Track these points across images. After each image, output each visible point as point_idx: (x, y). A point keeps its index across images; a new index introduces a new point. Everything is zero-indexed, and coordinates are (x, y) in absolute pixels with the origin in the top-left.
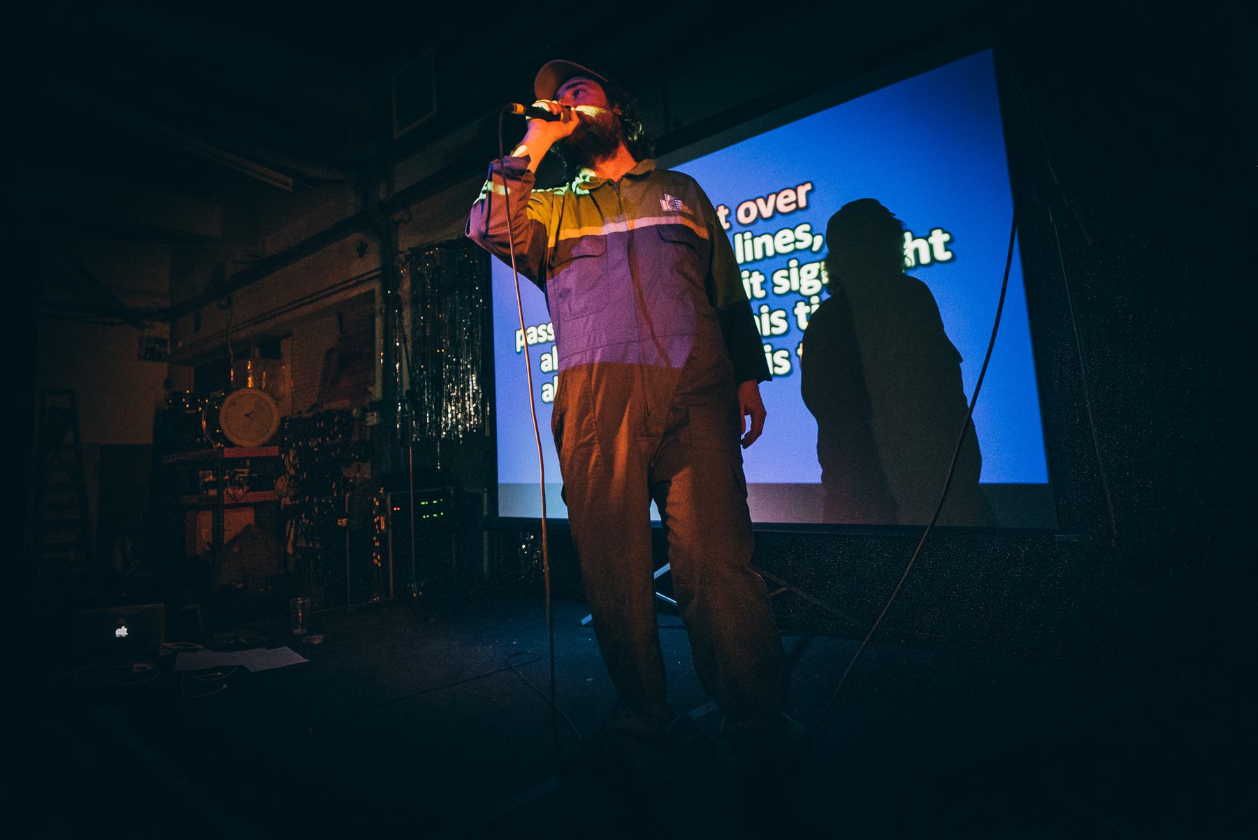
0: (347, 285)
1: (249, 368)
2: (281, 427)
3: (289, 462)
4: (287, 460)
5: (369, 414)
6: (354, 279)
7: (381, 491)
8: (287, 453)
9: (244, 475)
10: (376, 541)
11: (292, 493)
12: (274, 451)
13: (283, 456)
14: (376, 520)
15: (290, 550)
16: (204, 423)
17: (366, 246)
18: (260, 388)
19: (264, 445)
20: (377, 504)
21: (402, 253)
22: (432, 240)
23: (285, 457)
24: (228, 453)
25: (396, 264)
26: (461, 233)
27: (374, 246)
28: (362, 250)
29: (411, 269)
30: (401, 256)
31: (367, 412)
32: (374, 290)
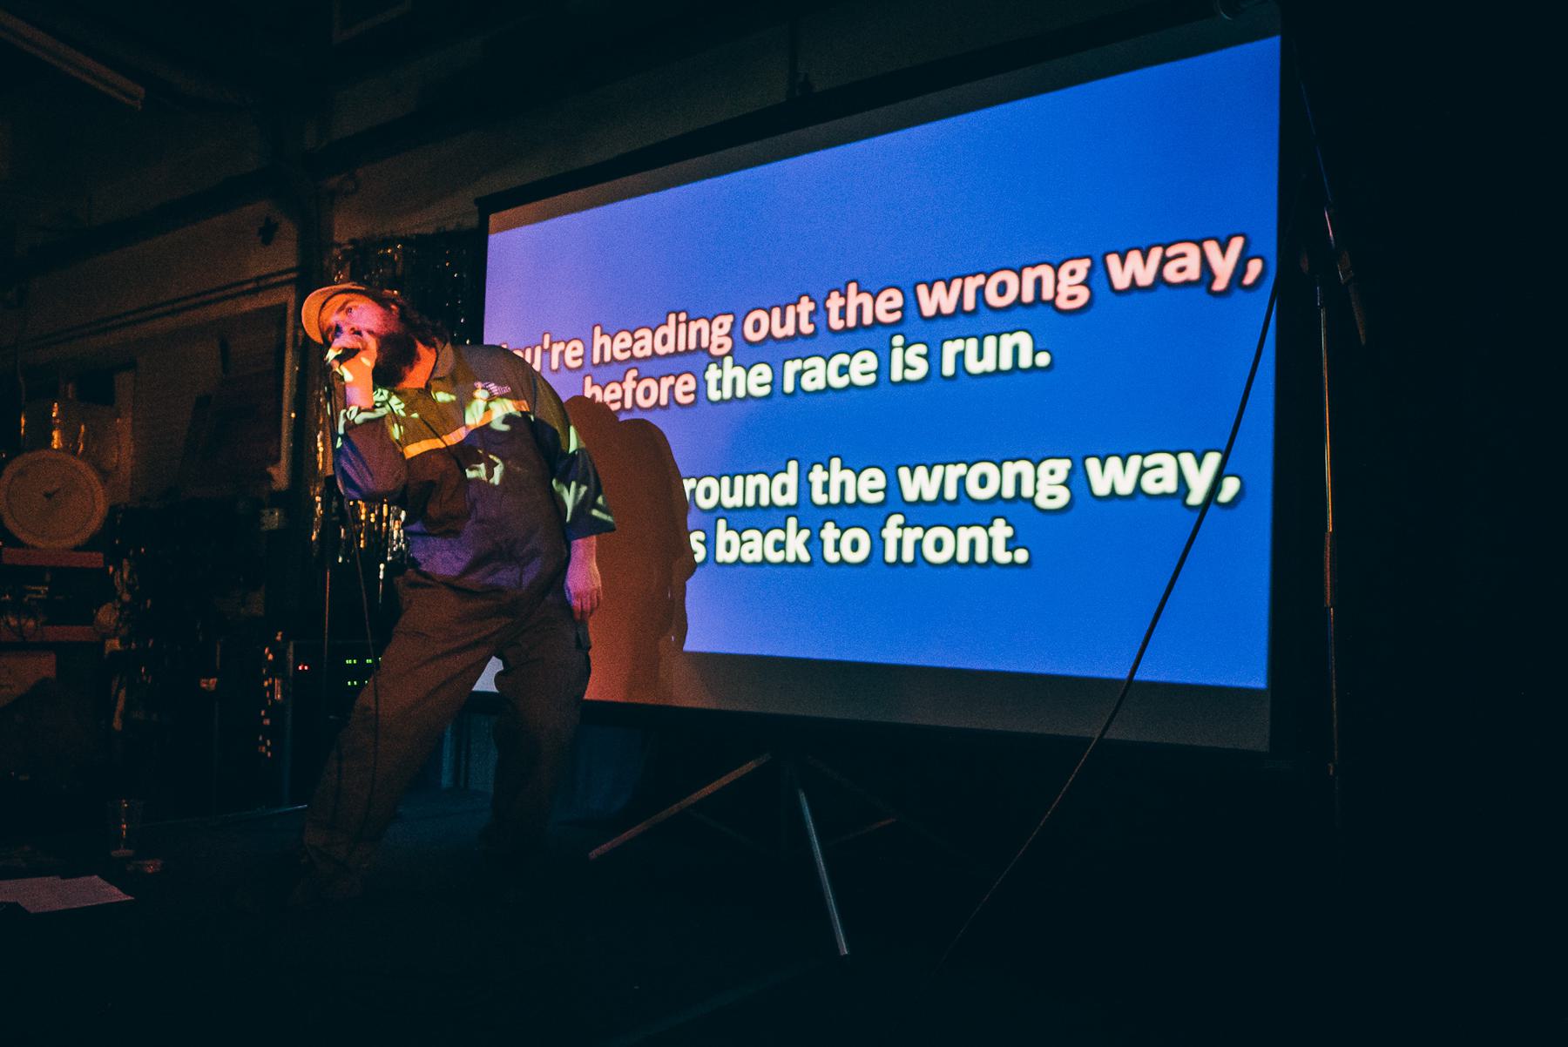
1: (54, 415)
3: (122, 579)
4: (117, 580)
5: (266, 512)
7: (279, 638)
8: (119, 567)
9: (39, 596)
10: (265, 717)
11: (124, 631)
12: (95, 559)
13: (111, 569)
14: (266, 684)
15: (117, 724)
18: (75, 452)
19: (77, 549)
20: (270, 657)
21: (339, 245)
22: (392, 232)
23: (114, 572)
24: (12, 556)
25: (326, 263)
27: (288, 231)
28: (268, 233)
32: (286, 304)
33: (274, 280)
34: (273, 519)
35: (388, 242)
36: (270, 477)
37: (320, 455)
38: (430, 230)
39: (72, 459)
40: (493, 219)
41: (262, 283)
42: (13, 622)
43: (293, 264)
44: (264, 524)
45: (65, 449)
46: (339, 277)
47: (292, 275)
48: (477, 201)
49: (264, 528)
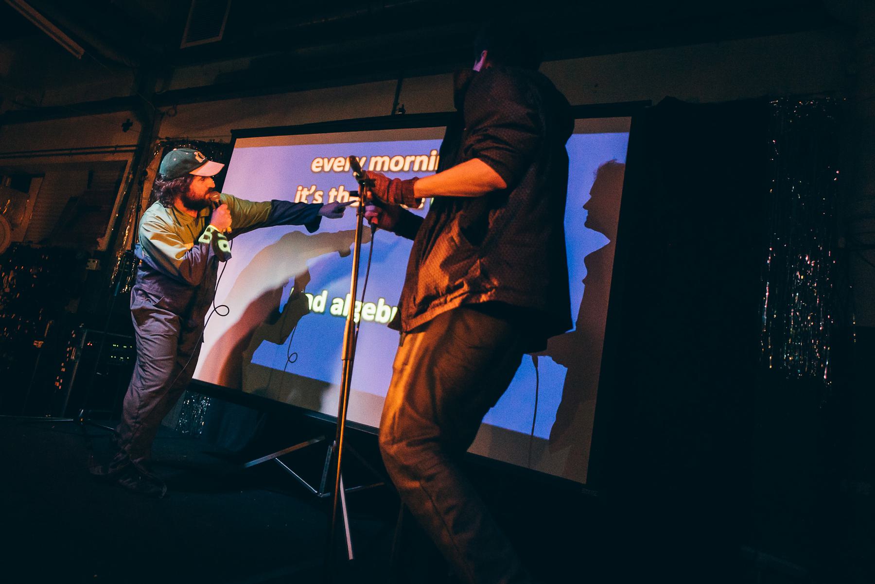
0: (106, 150)
2: (9, 249)
3: (8, 281)
4: (5, 281)
5: (92, 260)
6: (112, 147)
10: (63, 367)
13: (3, 274)
17: (131, 124)
21: (160, 139)
22: (188, 137)
23: (5, 275)
25: (152, 145)
26: (213, 139)
27: (137, 127)
28: (127, 126)
31: (90, 258)
34: (93, 265)
36: (97, 243)
37: (126, 237)
38: (207, 140)
41: (118, 149)
43: (135, 143)
44: (88, 267)
46: (156, 153)
47: (135, 148)
48: (232, 131)
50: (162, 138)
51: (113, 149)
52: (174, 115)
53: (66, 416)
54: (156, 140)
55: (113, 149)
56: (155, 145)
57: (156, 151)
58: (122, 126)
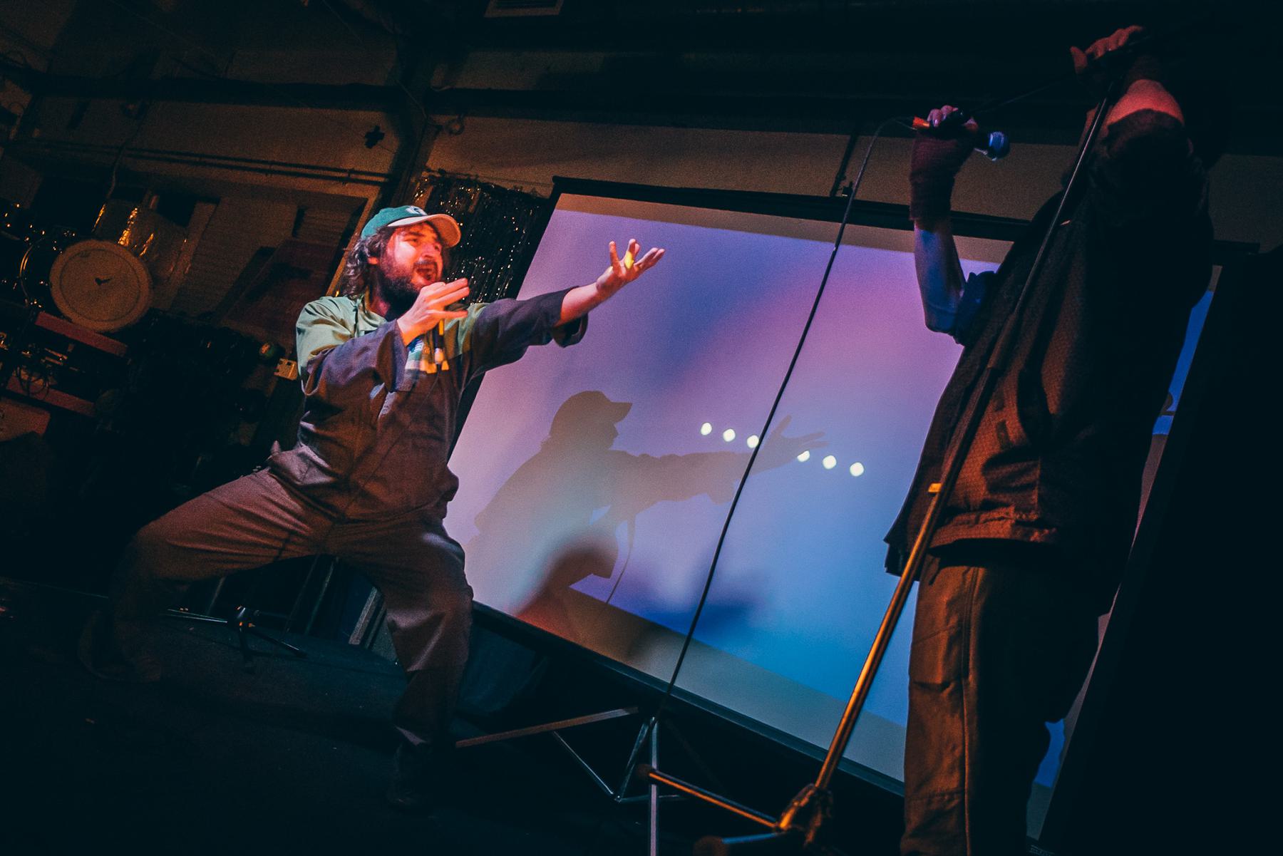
6: (345, 171)
16: (25, 262)
19: (107, 334)
21: (429, 170)
22: (477, 176)
24: (45, 320)
25: (413, 180)
27: (391, 143)
28: (373, 138)
29: (430, 198)
30: (425, 174)
32: (367, 199)
33: (364, 177)
35: (470, 183)
39: (132, 259)
40: (564, 198)
41: (353, 176)
42: (25, 376)
43: (385, 170)
45: (129, 248)
46: (419, 195)
47: (381, 180)
48: (555, 179)
49: (279, 374)
50: (432, 169)
51: (344, 175)
52: (459, 133)
53: (214, 615)
54: (423, 171)
55: (344, 175)
56: (416, 182)
57: (419, 192)
58: (367, 136)
